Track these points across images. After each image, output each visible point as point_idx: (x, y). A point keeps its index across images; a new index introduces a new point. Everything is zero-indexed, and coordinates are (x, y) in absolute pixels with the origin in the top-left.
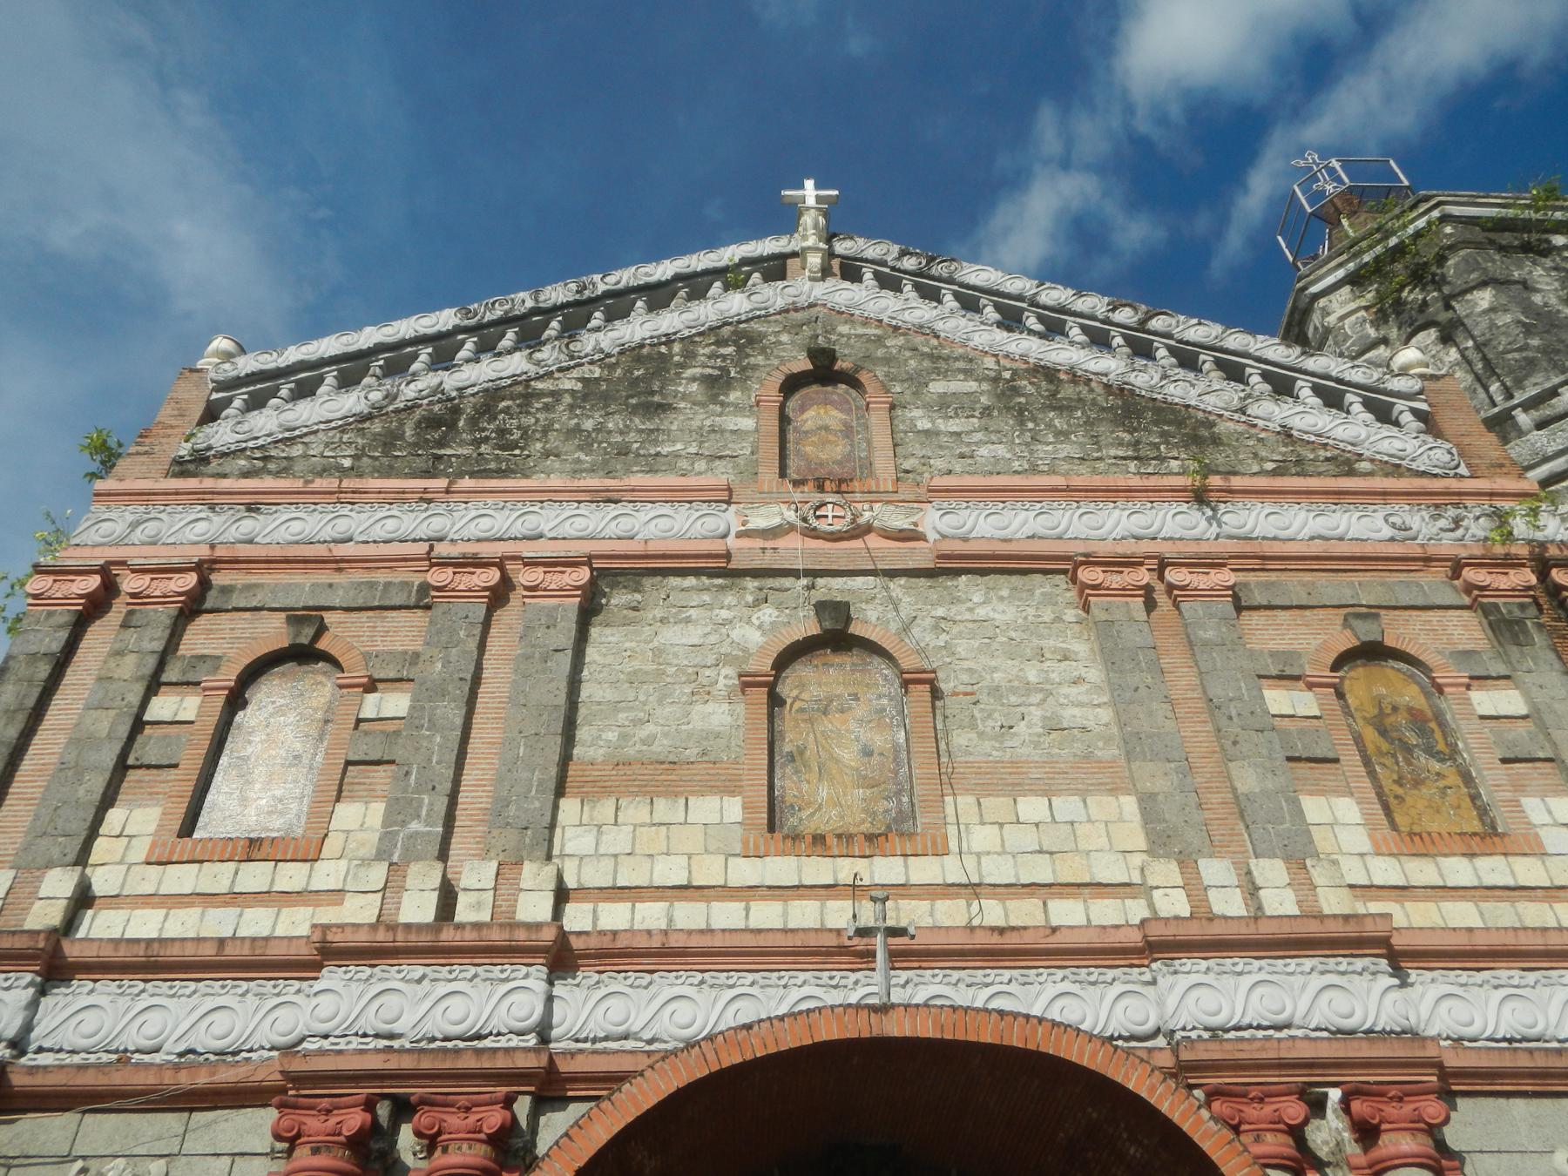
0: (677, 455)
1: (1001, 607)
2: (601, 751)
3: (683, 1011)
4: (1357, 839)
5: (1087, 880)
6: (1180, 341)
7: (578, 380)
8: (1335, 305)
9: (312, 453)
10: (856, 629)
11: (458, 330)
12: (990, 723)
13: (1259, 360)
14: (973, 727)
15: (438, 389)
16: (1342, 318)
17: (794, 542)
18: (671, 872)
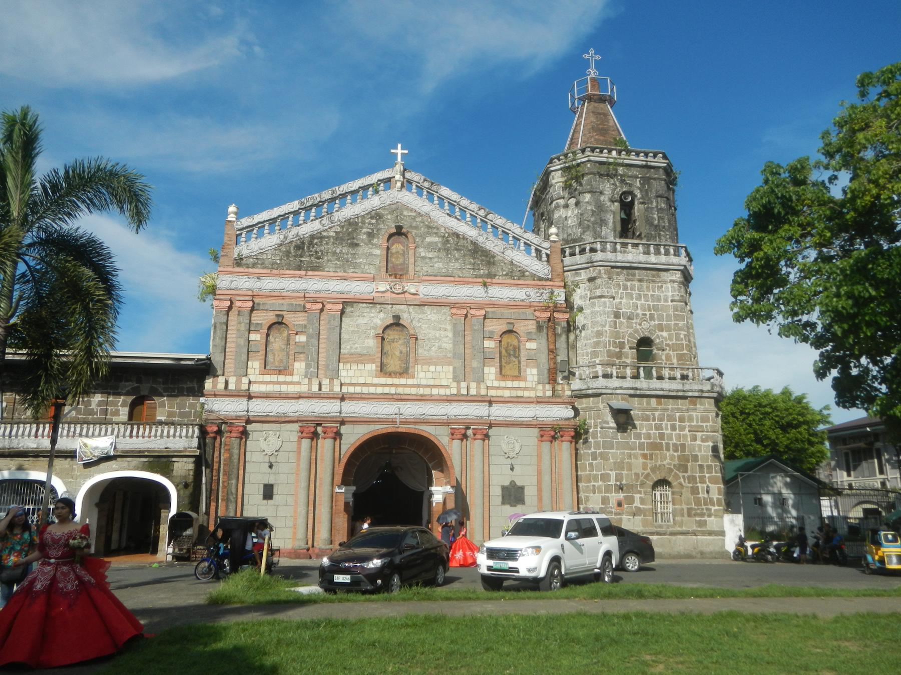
0: (360, 263)
1: (433, 315)
3: (364, 409)
4: (492, 377)
7: (335, 232)
8: (556, 177)
10: (401, 322)
11: (300, 209)
15: (298, 235)
16: (556, 183)
17: (388, 295)
18: (362, 381)
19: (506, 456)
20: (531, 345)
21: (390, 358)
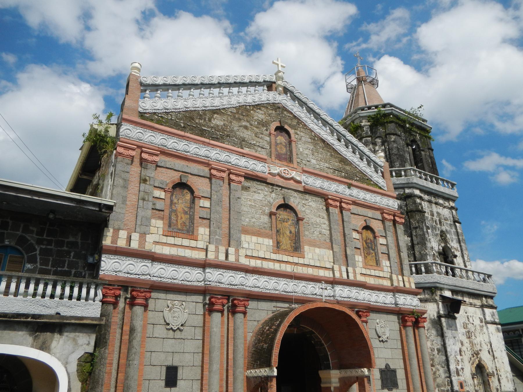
2: (246, 223)
4: (361, 264)
5: (324, 266)
6: (347, 139)
7: (231, 112)
9: (173, 119)
12: (311, 230)
13: (359, 149)
14: (308, 231)
19: (381, 339)
20: (382, 241)
21: (282, 236)
